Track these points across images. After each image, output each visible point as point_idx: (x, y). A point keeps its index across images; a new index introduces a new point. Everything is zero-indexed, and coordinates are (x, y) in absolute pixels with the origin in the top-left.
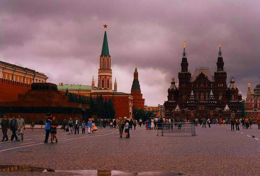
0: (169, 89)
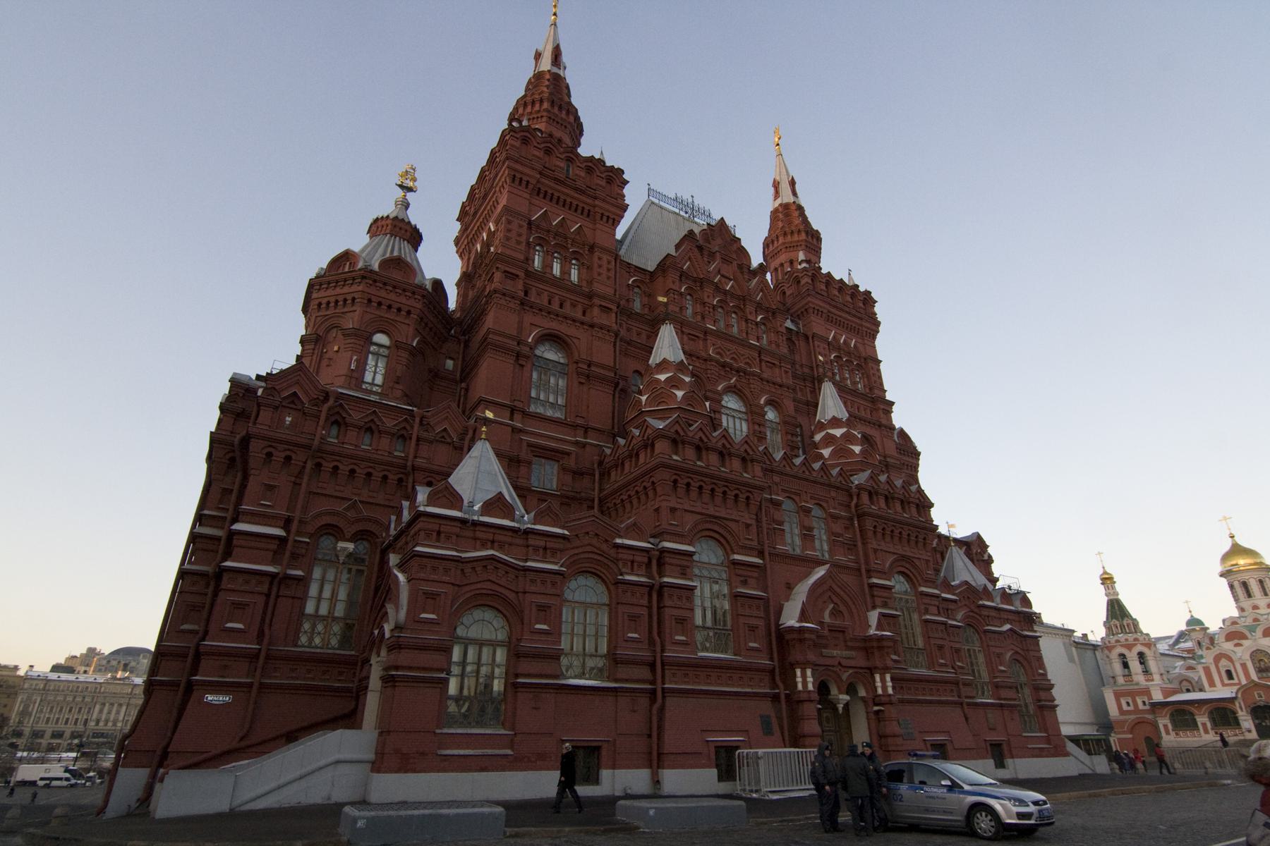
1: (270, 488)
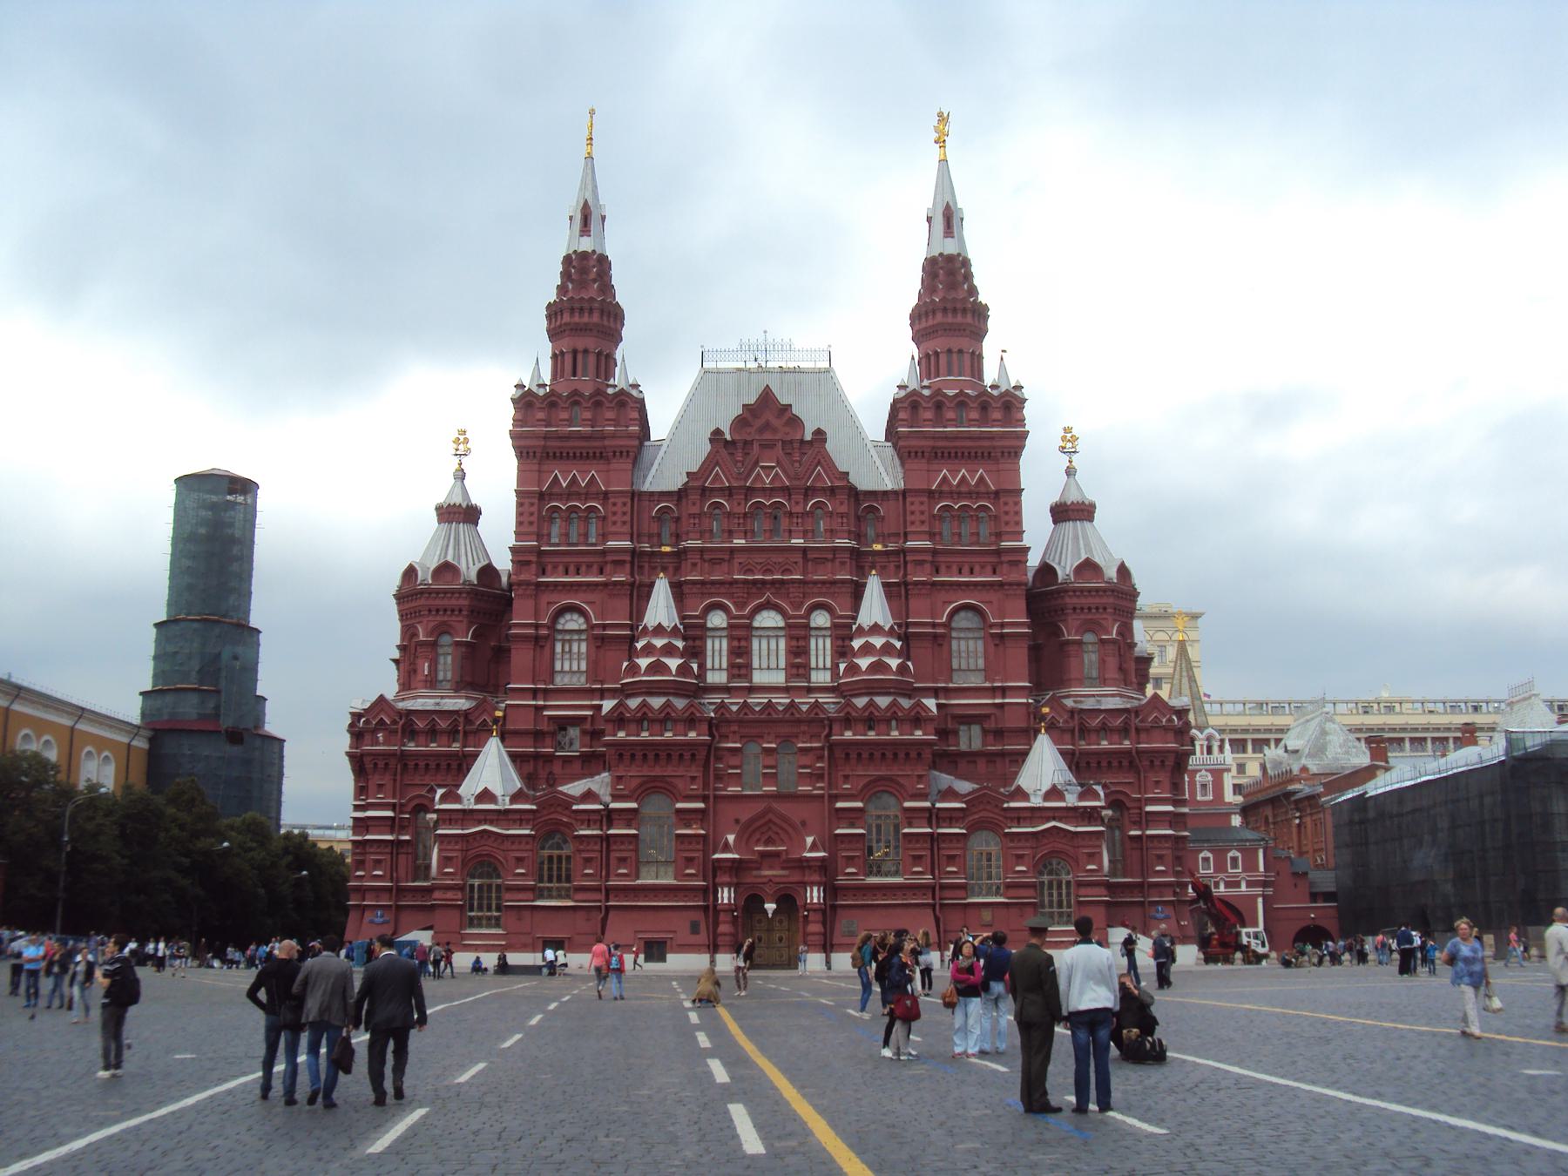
0: (410, 572)
1: (380, 786)
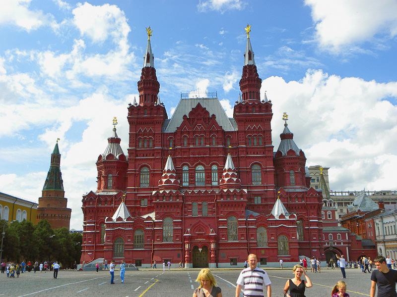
0: (100, 157)
